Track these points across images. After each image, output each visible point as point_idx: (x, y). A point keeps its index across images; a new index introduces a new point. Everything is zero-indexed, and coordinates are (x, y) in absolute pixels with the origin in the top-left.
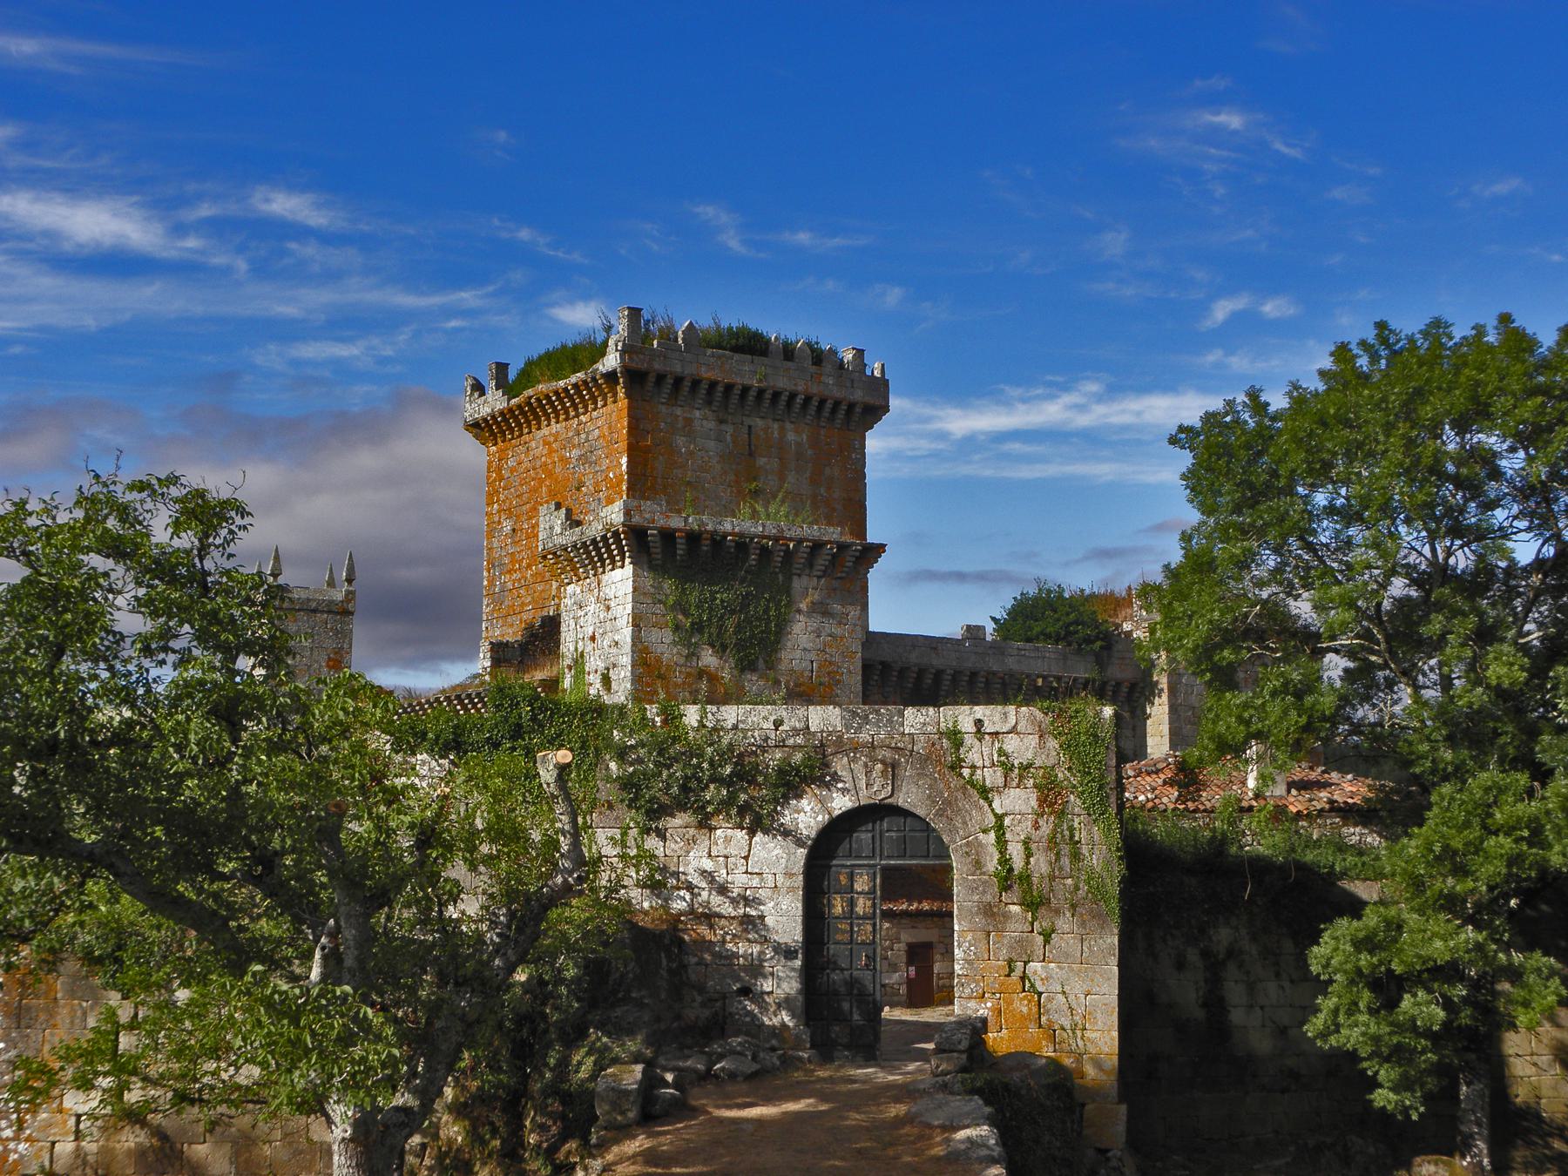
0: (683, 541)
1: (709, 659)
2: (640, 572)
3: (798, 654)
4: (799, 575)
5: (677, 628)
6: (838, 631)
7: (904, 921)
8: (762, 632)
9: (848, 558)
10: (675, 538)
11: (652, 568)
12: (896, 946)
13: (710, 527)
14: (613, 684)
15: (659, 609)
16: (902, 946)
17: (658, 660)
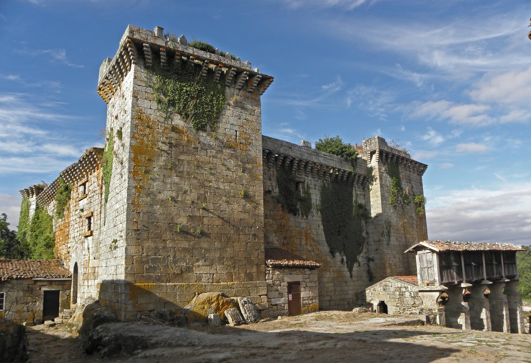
0: (165, 54)
1: (178, 121)
2: (139, 68)
3: (229, 126)
4: (229, 86)
5: (160, 102)
6: (250, 118)
7: (286, 271)
8: (209, 111)
9: (255, 81)
10: (160, 51)
11: (146, 68)
12: (282, 284)
13: (180, 49)
14: (123, 136)
15: (149, 90)
16: (285, 284)
17: (148, 118)
